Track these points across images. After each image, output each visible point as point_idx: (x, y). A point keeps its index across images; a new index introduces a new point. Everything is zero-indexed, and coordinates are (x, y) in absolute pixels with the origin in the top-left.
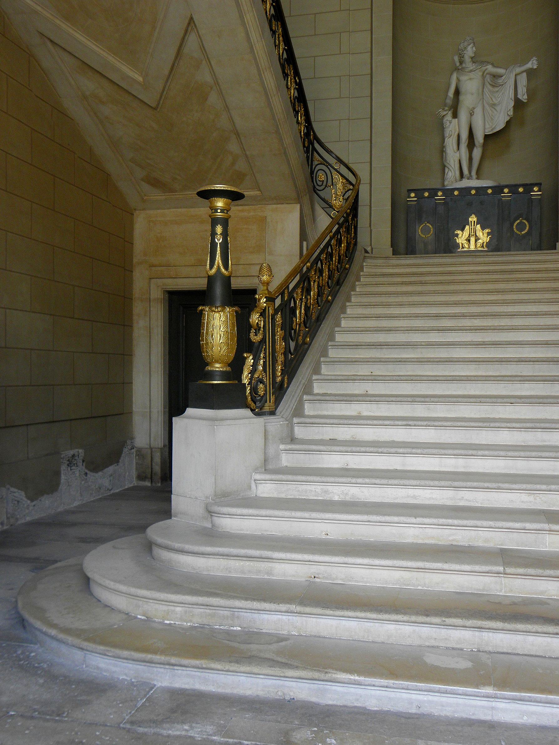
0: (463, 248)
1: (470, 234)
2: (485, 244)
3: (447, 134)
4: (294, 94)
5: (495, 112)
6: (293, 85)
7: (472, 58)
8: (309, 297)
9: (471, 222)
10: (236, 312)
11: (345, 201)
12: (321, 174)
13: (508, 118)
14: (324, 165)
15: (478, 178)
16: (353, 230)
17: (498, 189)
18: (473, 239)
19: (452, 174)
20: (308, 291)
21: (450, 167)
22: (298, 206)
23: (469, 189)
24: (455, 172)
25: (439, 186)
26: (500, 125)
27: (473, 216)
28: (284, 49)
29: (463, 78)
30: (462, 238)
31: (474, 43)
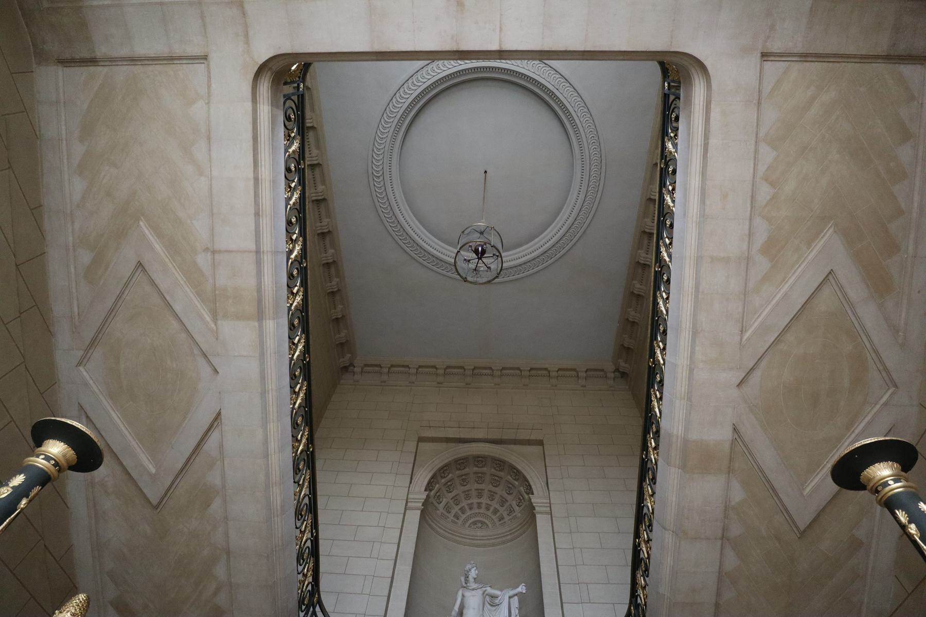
7: (475, 579)
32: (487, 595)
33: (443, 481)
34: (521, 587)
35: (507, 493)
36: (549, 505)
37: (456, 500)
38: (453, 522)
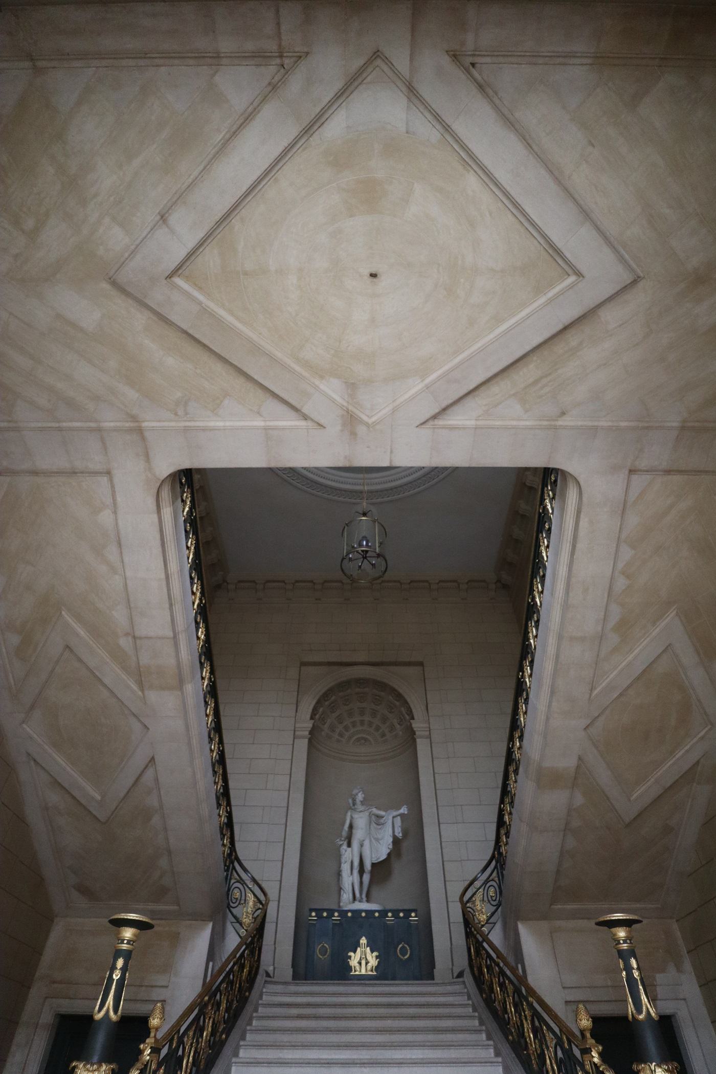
0: (355, 971)
2: (374, 968)
3: (343, 860)
4: (224, 820)
5: (379, 845)
6: (225, 813)
7: (361, 802)
8: (200, 1040)
9: (362, 944)
10: (113, 1070)
11: (254, 920)
12: (236, 891)
13: (389, 851)
14: (240, 883)
15: (368, 901)
16: (257, 952)
17: (383, 913)
18: (363, 962)
19: (346, 896)
20: (202, 1030)
21: (345, 890)
22: (210, 925)
23: (360, 911)
24: (349, 895)
25: (335, 907)
26: (383, 857)
27: (364, 938)
28: (222, 785)
29: (356, 816)
30: (354, 961)
31: (363, 791)
33: (327, 703)
34: (402, 809)
35: (388, 712)
36: (428, 729)
37: (340, 720)
38: (338, 741)
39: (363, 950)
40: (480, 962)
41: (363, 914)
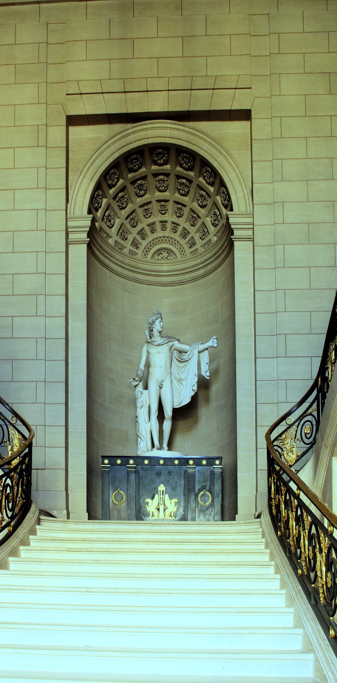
1: (159, 503)
3: (139, 404)
9: (160, 491)
23: (158, 459)
27: (162, 485)
32: (175, 349)
34: (211, 341)
39: (162, 496)
40: (279, 499)
41: (162, 462)
